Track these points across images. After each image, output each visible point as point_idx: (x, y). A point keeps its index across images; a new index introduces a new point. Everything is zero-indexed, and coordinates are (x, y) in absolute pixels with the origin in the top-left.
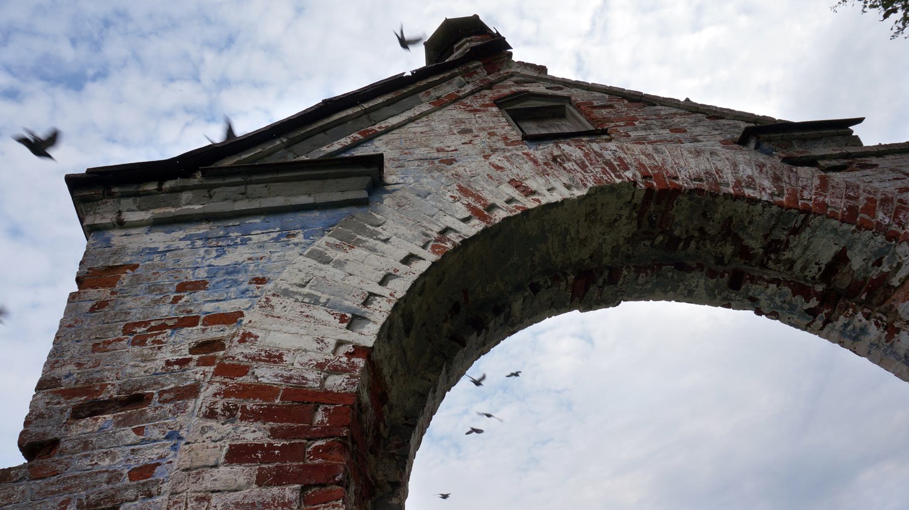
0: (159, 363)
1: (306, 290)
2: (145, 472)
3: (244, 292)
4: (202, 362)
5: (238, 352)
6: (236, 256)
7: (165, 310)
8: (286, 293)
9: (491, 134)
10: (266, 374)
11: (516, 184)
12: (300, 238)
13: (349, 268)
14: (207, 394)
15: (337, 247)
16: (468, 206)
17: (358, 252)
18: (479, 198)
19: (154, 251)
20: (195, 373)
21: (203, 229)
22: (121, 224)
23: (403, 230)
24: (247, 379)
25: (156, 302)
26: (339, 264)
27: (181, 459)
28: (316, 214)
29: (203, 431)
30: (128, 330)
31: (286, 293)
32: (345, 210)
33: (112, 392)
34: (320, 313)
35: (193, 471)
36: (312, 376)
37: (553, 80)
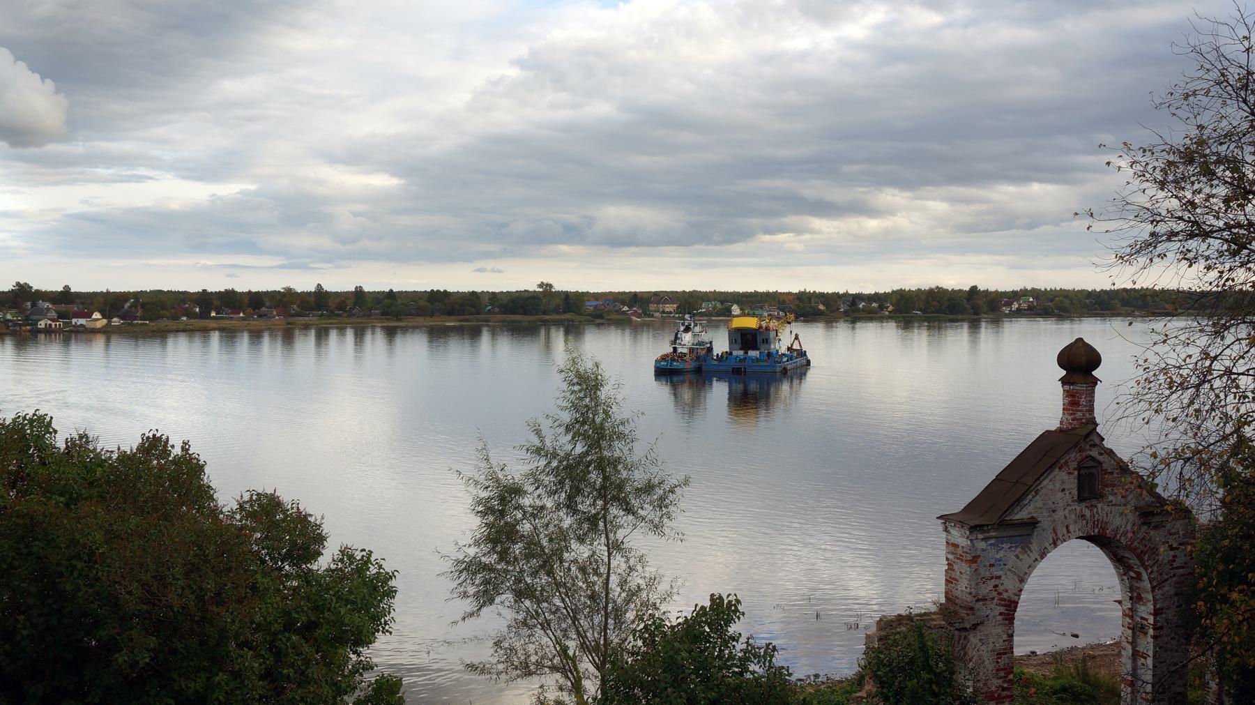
0: (987, 591)
1: (1013, 569)
2: (987, 616)
3: (1002, 568)
4: (995, 591)
5: (1001, 588)
6: (1001, 554)
7: (988, 574)
8: (1009, 570)
9: (1070, 493)
10: (1005, 595)
11: (1067, 527)
12: (1013, 549)
13: (1023, 561)
14: (996, 599)
15: (1020, 552)
16: (1053, 538)
17: (1026, 555)
18: (1057, 535)
19: (983, 550)
20: (995, 594)
21: (993, 541)
22: (977, 539)
23: (1036, 549)
24: (1002, 596)
25: (985, 570)
26: (1021, 560)
27: (992, 614)
28: (1018, 538)
29: (995, 608)
30: (982, 578)
31: (1009, 570)
32: (1025, 537)
33: (980, 597)
34: (1016, 578)
35: (994, 617)
36: (1012, 596)
37: (1103, 448)
